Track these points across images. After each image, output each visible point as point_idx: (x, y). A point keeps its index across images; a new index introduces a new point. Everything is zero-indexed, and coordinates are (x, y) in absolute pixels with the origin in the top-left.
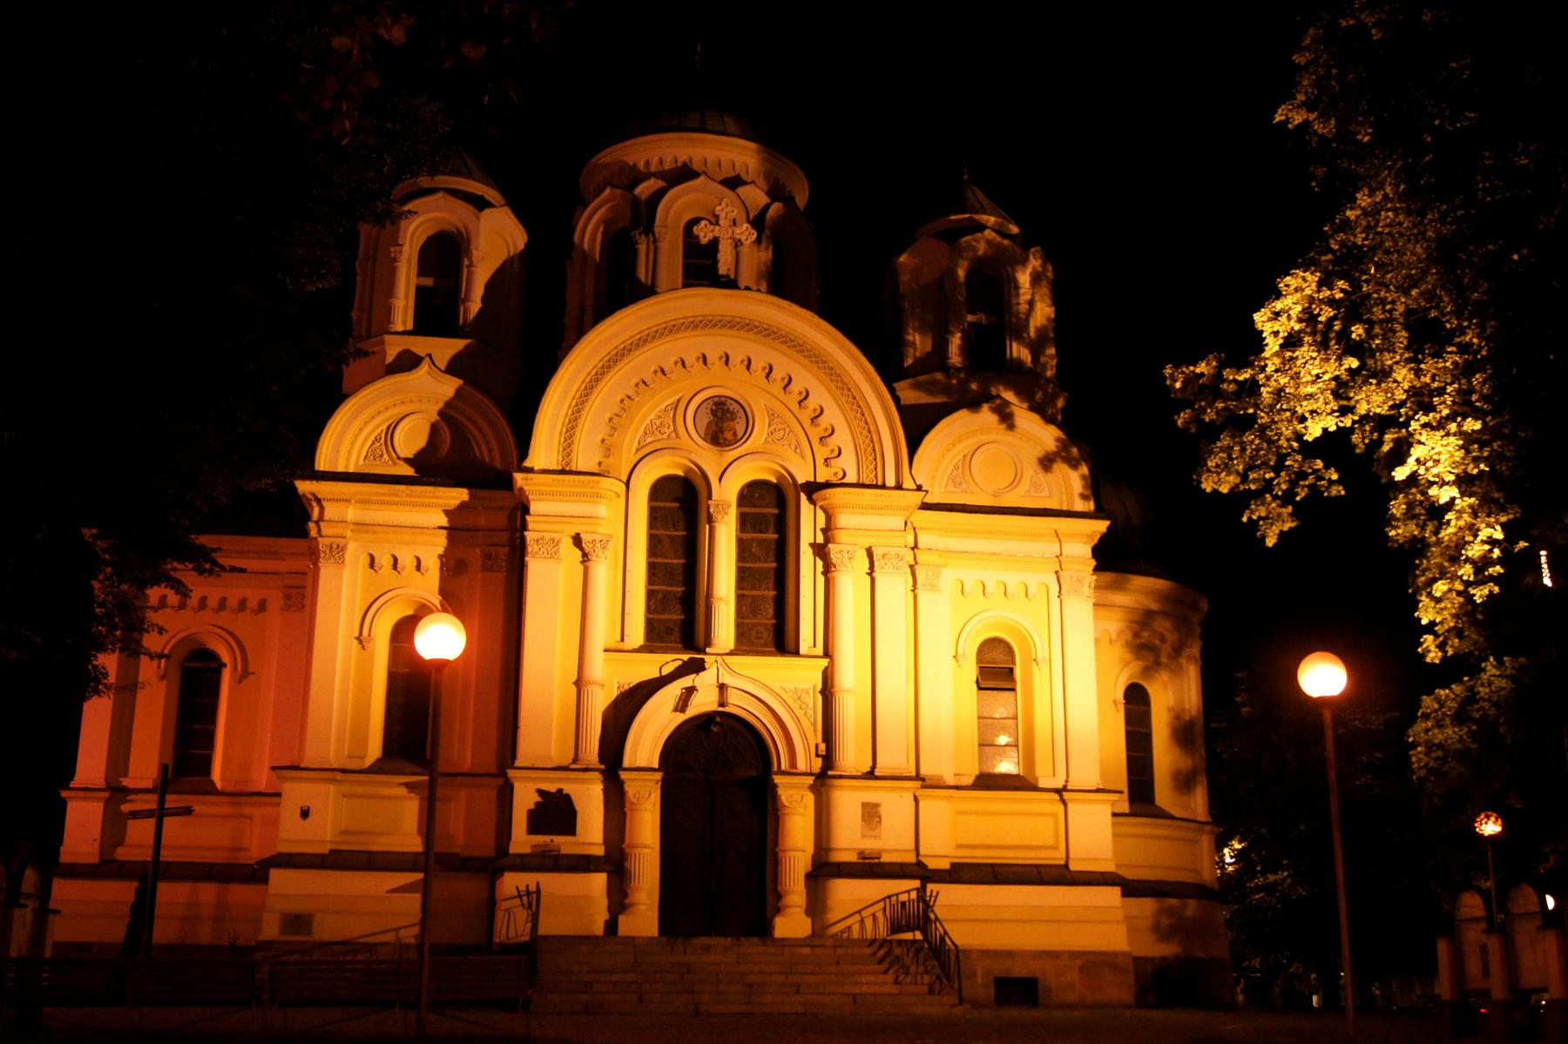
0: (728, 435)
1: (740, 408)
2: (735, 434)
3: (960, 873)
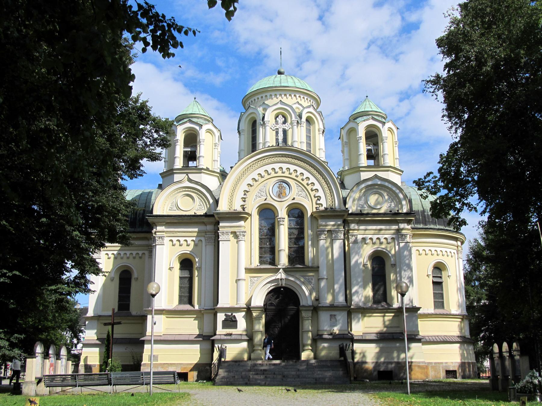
1: (286, 185)
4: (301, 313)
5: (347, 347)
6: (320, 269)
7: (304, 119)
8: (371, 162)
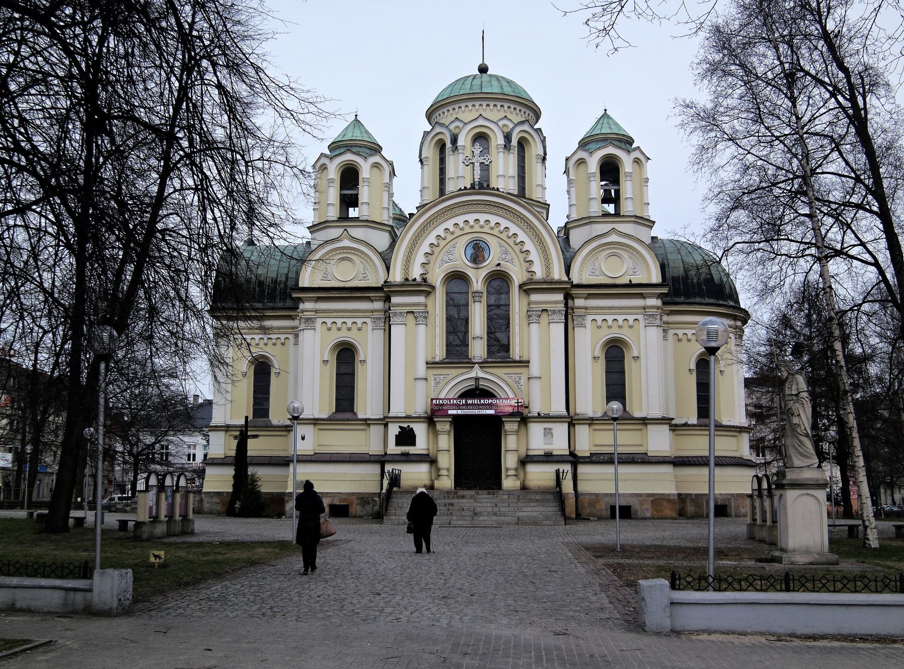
3: (595, 459)
5: (565, 474)
6: (531, 364)
7: (514, 142)
8: (611, 208)
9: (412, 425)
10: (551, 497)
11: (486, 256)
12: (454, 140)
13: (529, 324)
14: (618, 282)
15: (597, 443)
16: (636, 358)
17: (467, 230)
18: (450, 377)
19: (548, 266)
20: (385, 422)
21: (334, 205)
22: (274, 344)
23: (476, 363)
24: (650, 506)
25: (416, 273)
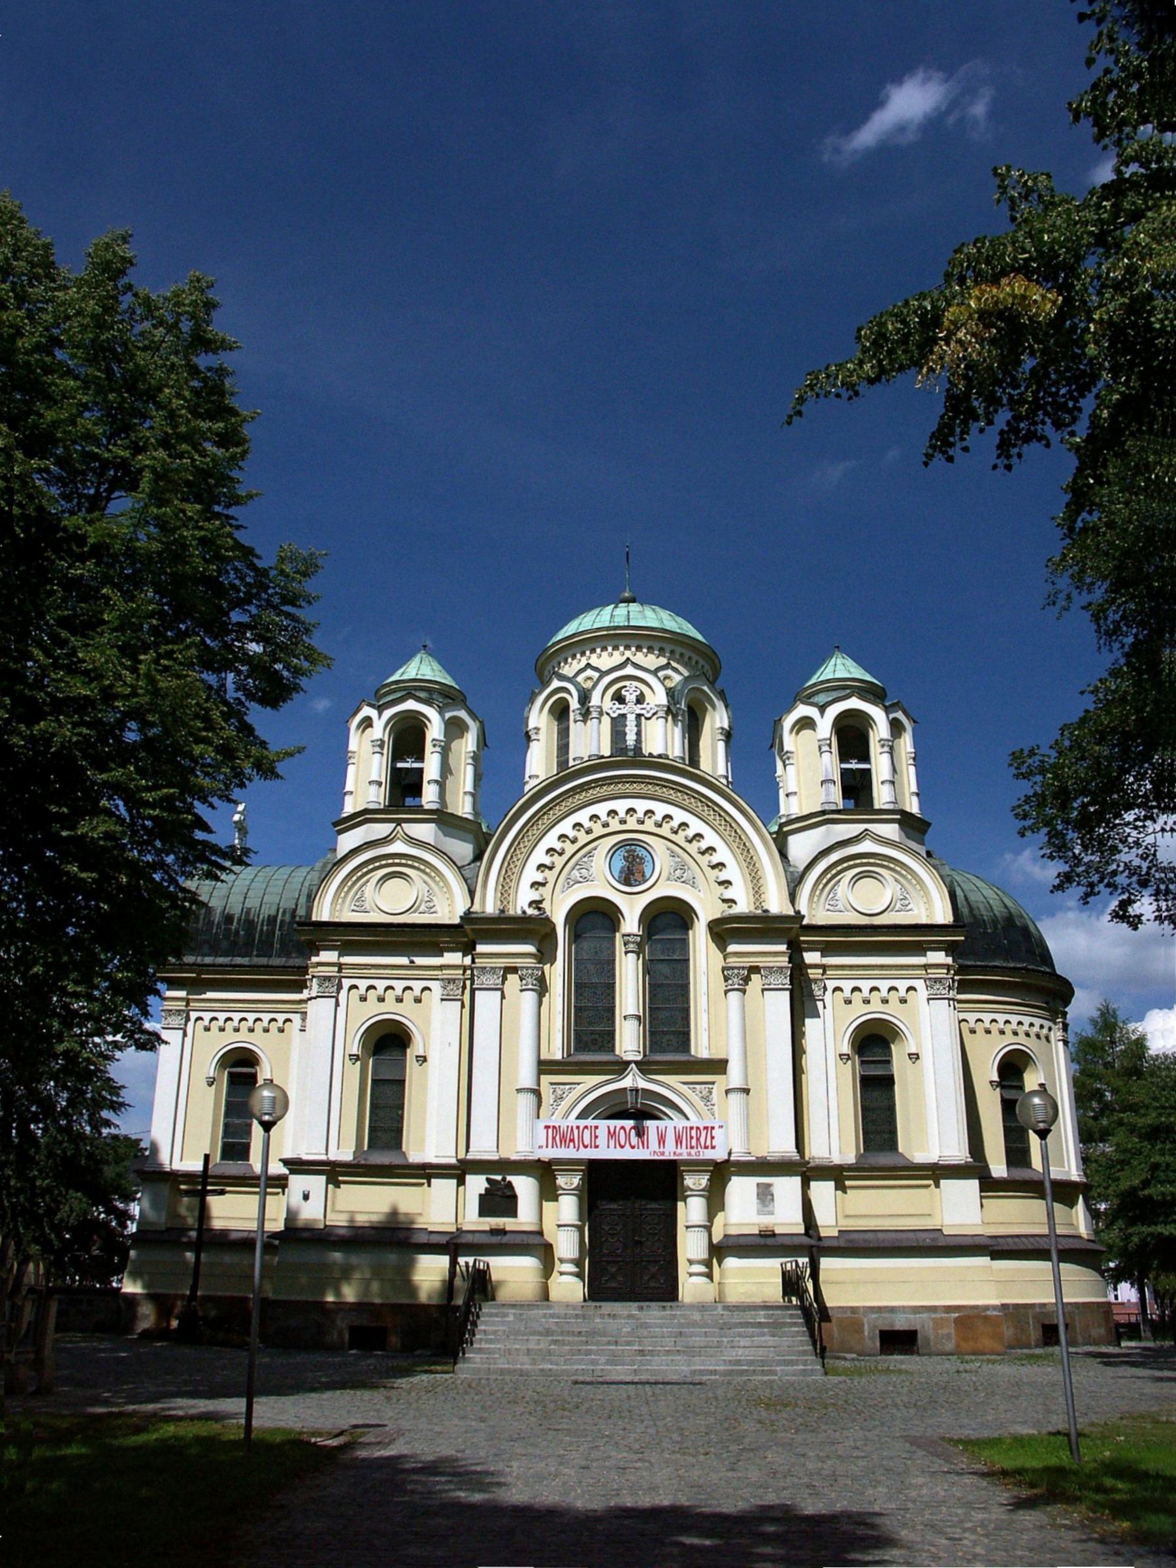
0: (638, 876)
2: (643, 876)
4: (683, 1179)
9: (509, 1178)
10: (786, 1317)
11: (648, 875)
12: (584, 697)
13: (726, 992)
14: (877, 921)
15: (851, 1213)
16: (915, 1057)
17: (615, 825)
18: (580, 1089)
19: (757, 890)
20: (460, 1171)
21: (380, 784)
22: (266, 1030)
23: (628, 1063)
24: (953, 1331)
25: (522, 901)
